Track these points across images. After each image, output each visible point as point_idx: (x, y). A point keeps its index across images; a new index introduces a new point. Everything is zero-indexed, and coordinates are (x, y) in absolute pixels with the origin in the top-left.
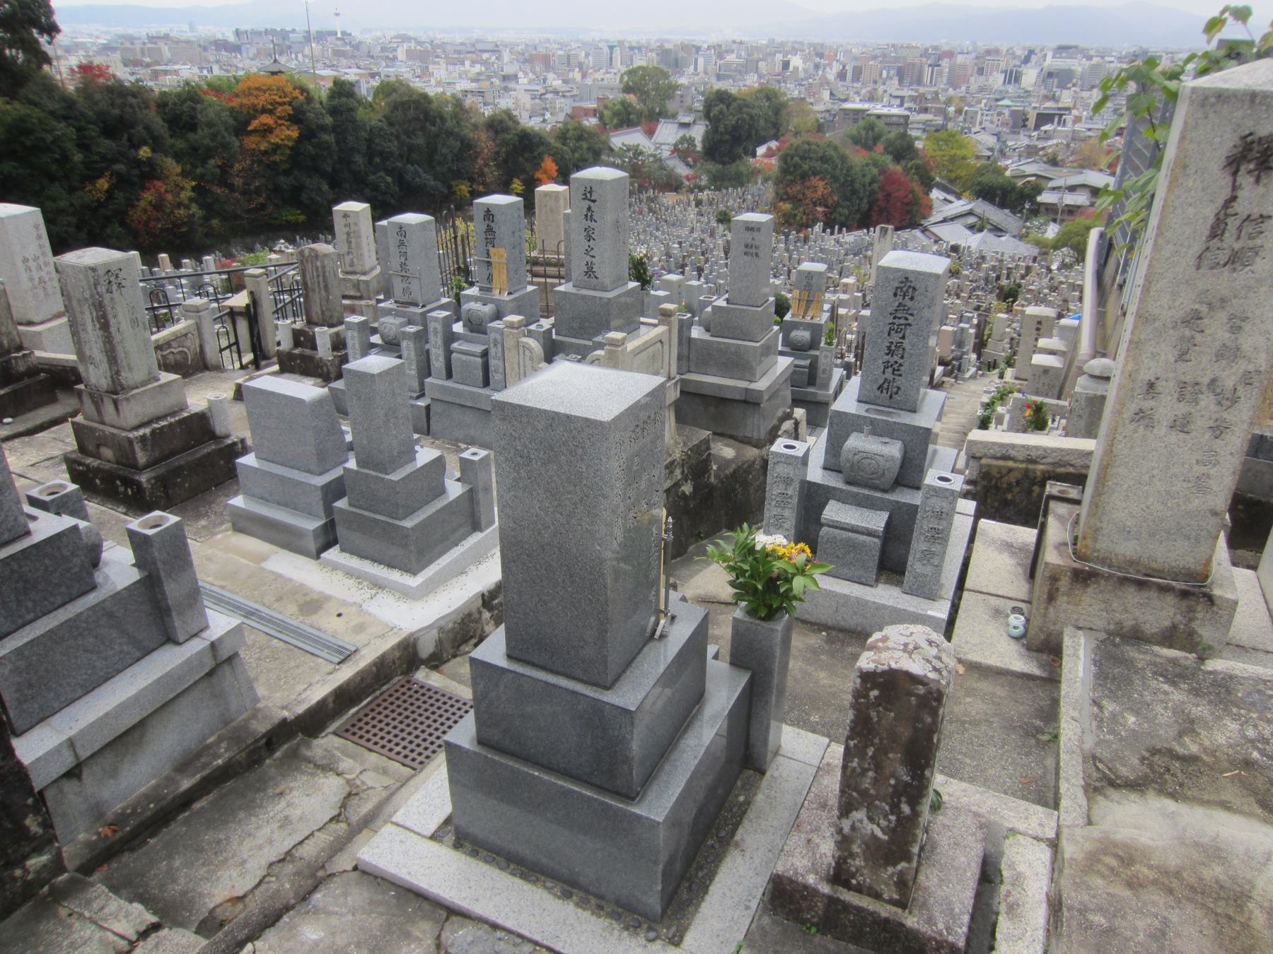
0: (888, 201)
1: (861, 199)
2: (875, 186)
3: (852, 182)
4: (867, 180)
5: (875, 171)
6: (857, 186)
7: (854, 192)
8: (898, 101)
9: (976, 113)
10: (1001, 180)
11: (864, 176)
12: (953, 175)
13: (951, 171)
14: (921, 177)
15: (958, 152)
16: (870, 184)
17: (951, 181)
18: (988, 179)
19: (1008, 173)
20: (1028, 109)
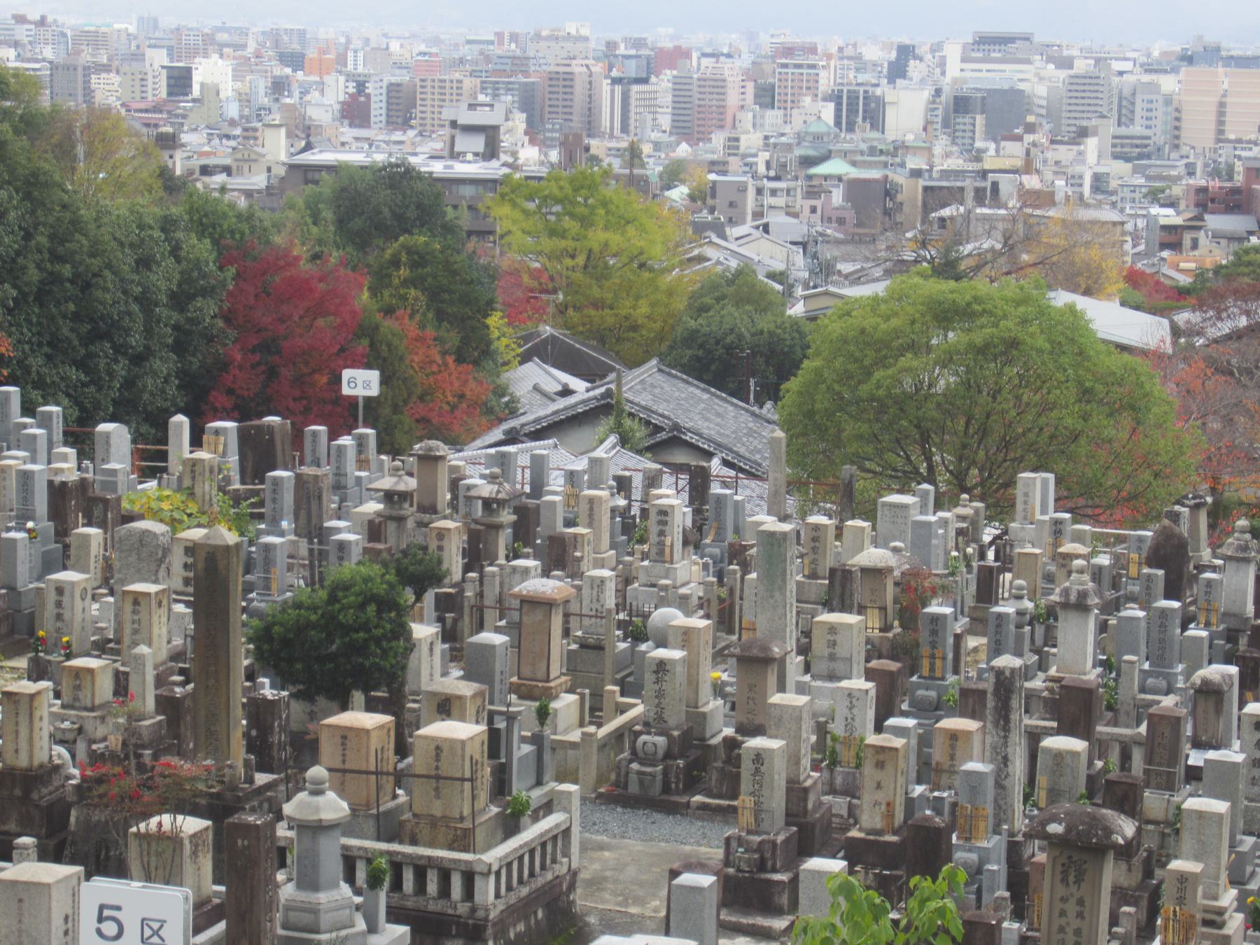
0: (272, 373)
1: (139, 359)
2: (207, 309)
3: (85, 284)
4: (163, 278)
5: (201, 248)
6: (107, 296)
7: (102, 329)
8: (478, 143)
9: (742, 189)
10: (765, 323)
11: (145, 263)
12: (608, 317)
13: (598, 305)
14: (434, 295)
15: (615, 239)
16: (180, 300)
17: (601, 338)
18: (733, 318)
19: (797, 310)
20: (899, 177)
